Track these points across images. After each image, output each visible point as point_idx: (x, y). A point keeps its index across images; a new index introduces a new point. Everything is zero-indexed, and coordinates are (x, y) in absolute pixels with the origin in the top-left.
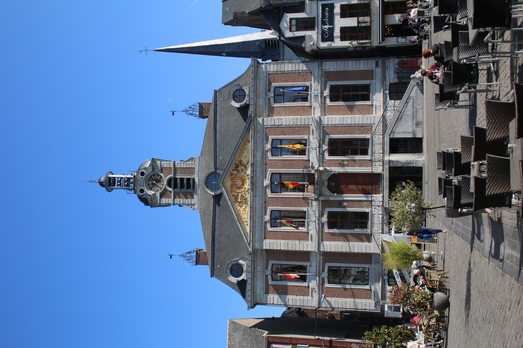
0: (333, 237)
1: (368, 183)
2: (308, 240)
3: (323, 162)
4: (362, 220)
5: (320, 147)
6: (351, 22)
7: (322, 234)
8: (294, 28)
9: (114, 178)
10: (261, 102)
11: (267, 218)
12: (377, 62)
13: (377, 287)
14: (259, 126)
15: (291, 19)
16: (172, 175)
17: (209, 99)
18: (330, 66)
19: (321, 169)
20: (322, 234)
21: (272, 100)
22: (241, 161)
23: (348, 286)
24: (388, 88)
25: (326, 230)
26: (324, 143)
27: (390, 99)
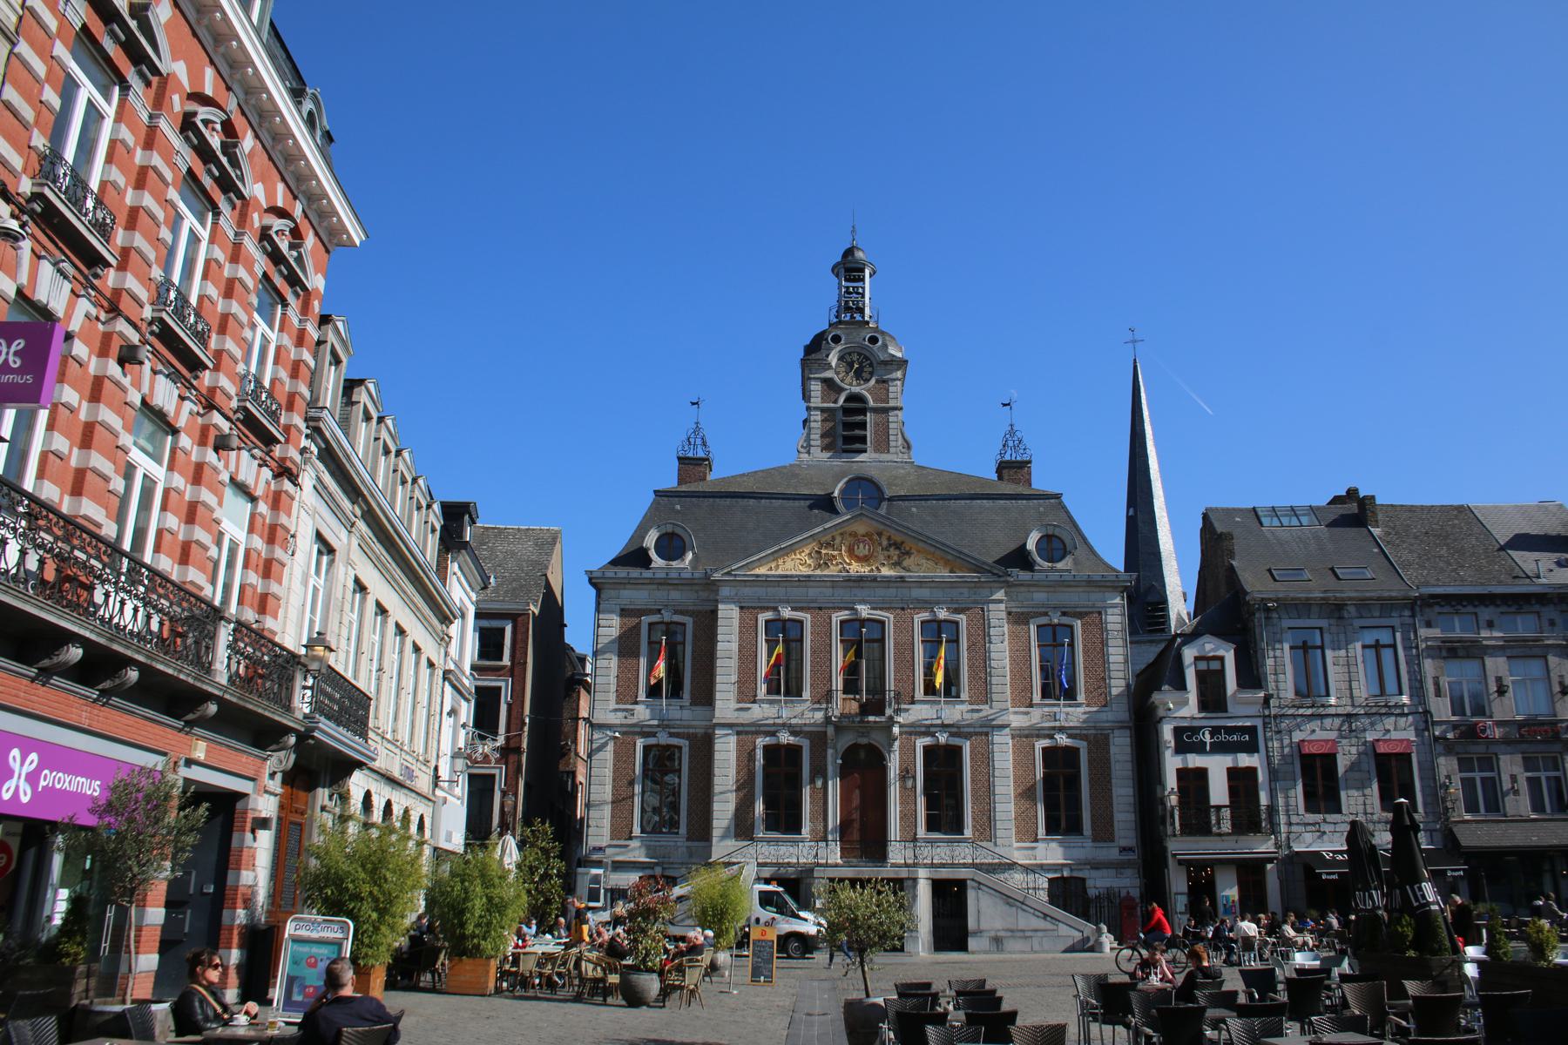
0: (746, 757)
1: (866, 835)
2: (739, 702)
3: (911, 734)
4: (785, 819)
5: (944, 726)
6: (1219, 792)
7: (753, 733)
8: (1203, 666)
9: (863, 280)
10: (1040, 596)
11: (787, 613)
12: (1130, 849)
13: (637, 853)
14: (986, 592)
15: (1221, 659)
16: (871, 403)
17: (1041, 480)
18: (1121, 748)
19: (896, 730)
20: (753, 733)
21: (1043, 620)
22: (908, 553)
23: (638, 789)
24: (1075, 874)
25: (761, 742)
26: (952, 735)
27: (1050, 880)
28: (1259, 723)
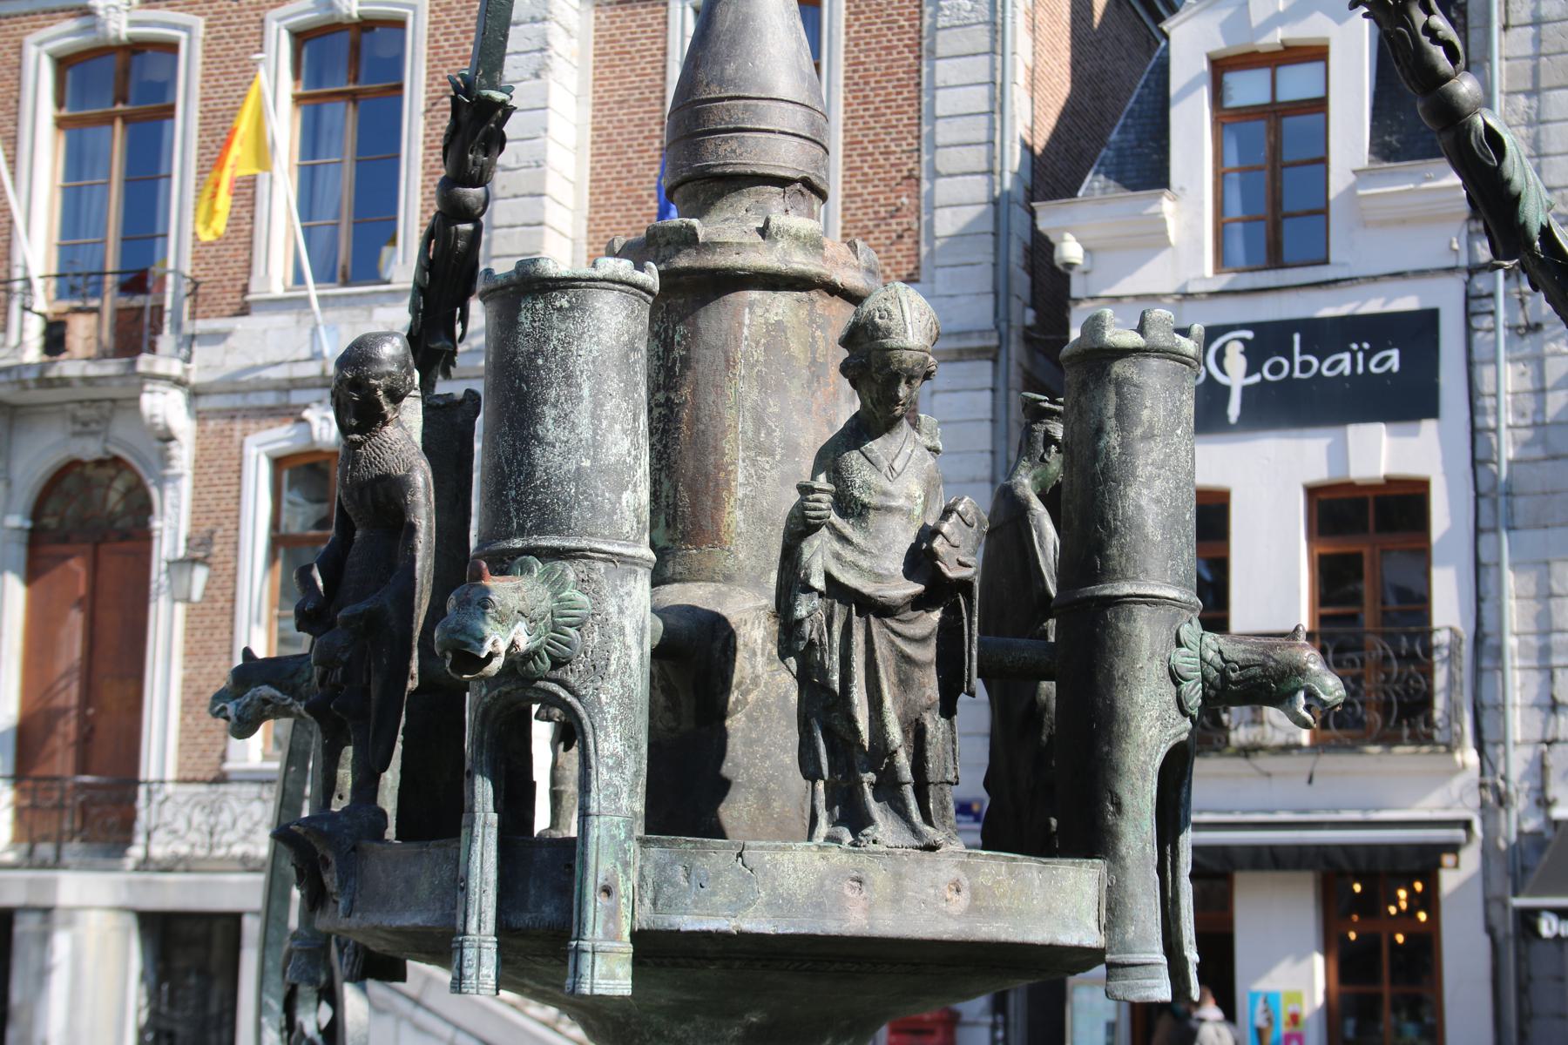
8: (1248, 89)
28: (1447, 298)
